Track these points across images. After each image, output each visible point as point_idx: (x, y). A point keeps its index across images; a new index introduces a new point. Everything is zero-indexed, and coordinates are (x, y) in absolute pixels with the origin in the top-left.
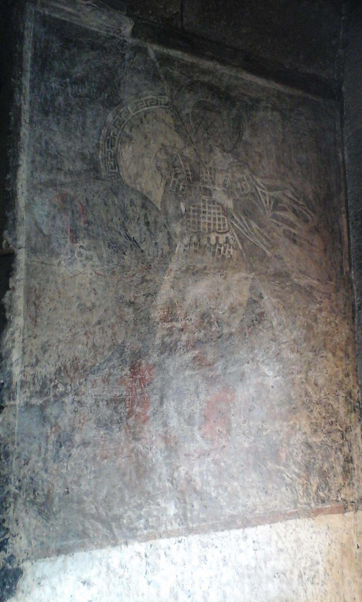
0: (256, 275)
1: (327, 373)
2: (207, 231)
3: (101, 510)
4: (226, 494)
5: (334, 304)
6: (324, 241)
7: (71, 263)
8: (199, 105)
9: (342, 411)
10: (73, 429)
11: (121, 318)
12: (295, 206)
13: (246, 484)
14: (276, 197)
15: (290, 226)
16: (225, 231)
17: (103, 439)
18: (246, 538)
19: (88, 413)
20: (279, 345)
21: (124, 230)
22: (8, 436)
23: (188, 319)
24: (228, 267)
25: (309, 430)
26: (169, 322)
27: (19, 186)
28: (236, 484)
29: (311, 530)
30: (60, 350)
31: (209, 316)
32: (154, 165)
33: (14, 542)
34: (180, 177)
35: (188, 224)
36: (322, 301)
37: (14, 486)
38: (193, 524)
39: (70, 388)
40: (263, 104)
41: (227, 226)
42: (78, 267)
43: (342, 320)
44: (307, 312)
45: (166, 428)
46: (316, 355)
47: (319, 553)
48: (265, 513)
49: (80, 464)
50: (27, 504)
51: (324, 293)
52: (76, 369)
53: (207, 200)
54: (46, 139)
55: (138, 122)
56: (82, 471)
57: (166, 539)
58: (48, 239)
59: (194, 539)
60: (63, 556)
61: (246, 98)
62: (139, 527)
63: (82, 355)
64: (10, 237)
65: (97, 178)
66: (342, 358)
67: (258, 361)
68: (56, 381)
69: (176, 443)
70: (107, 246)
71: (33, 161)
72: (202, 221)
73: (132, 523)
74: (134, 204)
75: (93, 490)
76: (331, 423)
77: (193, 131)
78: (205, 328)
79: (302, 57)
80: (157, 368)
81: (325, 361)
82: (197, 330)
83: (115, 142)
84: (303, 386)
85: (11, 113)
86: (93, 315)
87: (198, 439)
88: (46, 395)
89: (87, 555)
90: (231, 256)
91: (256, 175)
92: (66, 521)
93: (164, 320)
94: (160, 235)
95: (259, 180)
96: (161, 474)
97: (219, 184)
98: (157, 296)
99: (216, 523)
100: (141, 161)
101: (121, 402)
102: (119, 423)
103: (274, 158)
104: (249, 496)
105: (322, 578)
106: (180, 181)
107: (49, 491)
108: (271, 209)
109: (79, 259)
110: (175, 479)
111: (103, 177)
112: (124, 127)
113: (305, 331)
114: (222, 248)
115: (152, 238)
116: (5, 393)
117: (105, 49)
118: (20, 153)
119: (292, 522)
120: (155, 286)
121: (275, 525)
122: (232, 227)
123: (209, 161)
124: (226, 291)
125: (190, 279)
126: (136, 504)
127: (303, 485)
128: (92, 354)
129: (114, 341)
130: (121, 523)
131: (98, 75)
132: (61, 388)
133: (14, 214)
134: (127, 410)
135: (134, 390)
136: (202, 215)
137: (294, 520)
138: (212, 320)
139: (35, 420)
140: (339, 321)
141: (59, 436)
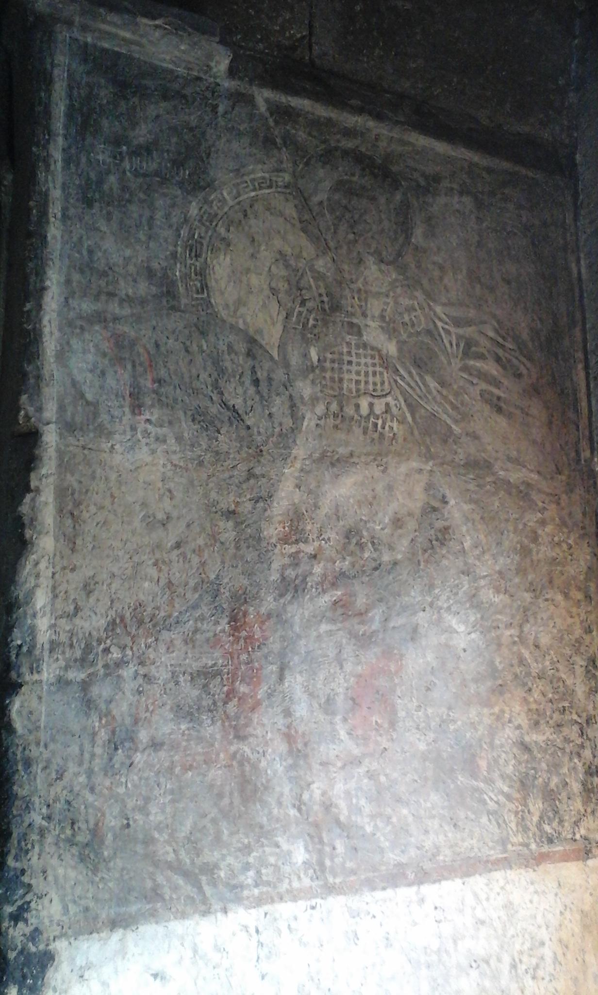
2: (354, 394)
3: (183, 854)
4: (389, 828)
5: (565, 513)
6: (548, 408)
7: (132, 448)
8: (339, 186)
9: (581, 690)
10: (136, 722)
11: (214, 536)
12: (500, 352)
13: (422, 812)
14: (467, 336)
15: (491, 384)
17: (186, 738)
20: (475, 580)
21: (218, 393)
22: (30, 731)
23: (323, 539)
25: (526, 721)
26: (292, 543)
27: (45, 321)
28: (405, 811)
29: (532, 889)
32: (266, 287)
33: (40, 907)
34: (309, 304)
35: (324, 382)
36: (544, 508)
37: (40, 814)
38: (334, 877)
39: (130, 653)
40: (445, 184)
42: (143, 454)
43: (579, 538)
44: (521, 527)
45: (290, 720)
46: (536, 597)
47: (544, 928)
48: (453, 861)
49: (147, 779)
50: (61, 845)
51: (548, 494)
52: (141, 623)
54: (89, 246)
55: (240, 215)
57: (290, 904)
58: (93, 407)
59: (336, 903)
60: (121, 931)
61: (416, 175)
62: (246, 882)
63: (151, 598)
64: (32, 406)
65: (173, 308)
66: (579, 601)
67: (441, 608)
68: (108, 641)
69: (306, 744)
71: (68, 282)
72: (346, 376)
75: (169, 821)
77: (330, 229)
78: (352, 554)
79: (508, 105)
80: (273, 620)
81: (552, 607)
83: (201, 248)
84: (515, 648)
85: (31, 203)
86: (168, 534)
87: (342, 738)
90: (394, 434)
91: (434, 301)
92: (125, 872)
93: (285, 540)
94: (278, 401)
95: (439, 309)
96: (282, 794)
97: (373, 317)
100: (244, 279)
101: (214, 676)
103: (464, 271)
104: (426, 832)
105: (550, 968)
106: (310, 311)
107: (96, 825)
108: (460, 355)
109: (144, 441)
110: (305, 804)
112: (216, 225)
113: (517, 558)
114: (380, 422)
115: (264, 406)
116: (24, 661)
117: (184, 97)
118: (47, 269)
119: (498, 875)
120: (269, 484)
121: (471, 880)
122: (394, 387)
123: (357, 280)
124: (386, 493)
125: (326, 473)
126: (240, 845)
127: (516, 813)
128: (166, 596)
129: (203, 576)
130: (215, 876)
131: (174, 140)
132: (116, 654)
133: (38, 367)
134: (225, 689)
135: (236, 656)
137: (503, 871)
138: (363, 540)
139: (73, 706)
140: (575, 541)
141: (113, 732)
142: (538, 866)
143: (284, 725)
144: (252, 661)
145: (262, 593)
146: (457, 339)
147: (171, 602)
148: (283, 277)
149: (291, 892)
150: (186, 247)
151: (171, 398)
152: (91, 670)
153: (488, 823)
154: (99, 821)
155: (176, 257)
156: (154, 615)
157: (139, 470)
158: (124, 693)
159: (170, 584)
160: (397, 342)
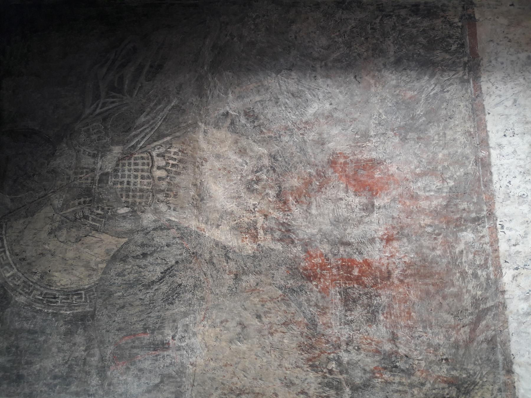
1: (315, 33)
2: (151, 180)
3: (466, 321)
4: (451, 168)
7: (192, 350)
9: (360, 15)
10: (377, 352)
11: (253, 290)
13: (441, 143)
16: (150, 157)
17: (389, 316)
18: (500, 145)
19: (360, 333)
21: (153, 285)
23: (254, 209)
24: (192, 155)
25: (380, 59)
26: (257, 232)
28: (440, 156)
29: (494, 62)
30: (290, 366)
32: (75, 246)
34: (87, 213)
35: (143, 204)
38: (483, 210)
39: (332, 354)
41: (145, 155)
42: (197, 341)
44: (244, 55)
45: (377, 239)
49: (416, 345)
52: (312, 347)
54: (51, 378)
55: (24, 263)
56: (423, 342)
57: (499, 244)
59: (500, 211)
62: (485, 276)
63: (295, 338)
65: (93, 316)
68: (325, 371)
69: (394, 228)
72: (139, 186)
73: (481, 285)
75: (444, 330)
76: (372, 30)
78: (264, 188)
80: (309, 248)
82: (266, 198)
83: (49, 294)
84: (330, 64)
86: (252, 325)
88: (341, 383)
89: (514, 339)
90: (180, 151)
92: (476, 362)
93: (255, 237)
94: (157, 240)
95: (88, 111)
96: (428, 248)
97: (94, 163)
98: (229, 247)
99: (483, 181)
100: (70, 262)
101: (347, 293)
102: (371, 296)
104: (454, 140)
107: (446, 382)
109: (187, 341)
110: (434, 230)
112: (32, 282)
114: (171, 162)
115: (161, 250)
120: (217, 248)
121: (487, 107)
123: (67, 175)
124: (221, 160)
125: (208, 205)
128: (294, 327)
129: (279, 299)
132: (333, 365)
134: (356, 286)
135: (334, 277)
138: (254, 179)
141: (385, 368)
142: (478, 57)
143: (380, 243)
144: (337, 265)
145: (291, 256)
146: (109, 97)
147: (298, 323)
148: (68, 232)
149: (492, 243)
150: (49, 305)
152: (344, 383)
153: (449, 93)
154: (443, 380)
155: (56, 313)
156: (306, 336)
157: (208, 345)
158: (359, 361)
159: (285, 324)
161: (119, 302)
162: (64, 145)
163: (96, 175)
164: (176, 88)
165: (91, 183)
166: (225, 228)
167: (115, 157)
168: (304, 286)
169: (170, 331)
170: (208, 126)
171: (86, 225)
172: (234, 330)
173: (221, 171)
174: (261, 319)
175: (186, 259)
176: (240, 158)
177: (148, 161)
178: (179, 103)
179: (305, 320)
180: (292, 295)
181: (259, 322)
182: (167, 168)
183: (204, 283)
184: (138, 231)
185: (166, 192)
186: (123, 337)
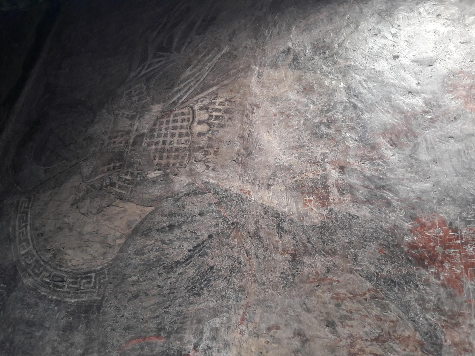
0: (255, 62)
2: (190, 137)
16: (191, 112)
21: (177, 267)
23: (323, 160)
24: (241, 103)
26: (327, 192)
31: (317, 126)
32: (95, 218)
34: (115, 179)
41: (186, 110)
53: (148, 140)
65: (99, 308)
70: (197, 298)
72: (175, 145)
74: (141, 250)
78: (339, 131)
86: (319, 337)
90: (226, 100)
95: (133, 74)
100: (87, 237)
108: (168, 54)
111: (99, 298)
112: (44, 261)
114: (215, 114)
115: (192, 221)
120: (266, 216)
123: (102, 140)
124: (277, 103)
136: (167, 147)
138: (325, 121)
148: (91, 202)
151: (177, 318)
155: (60, 301)
160: (152, 104)
161: (132, 289)
162: (105, 111)
163: (131, 137)
164: (229, 35)
165: (124, 146)
166: (278, 187)
167: (153, 116)
168: (413, 275)
169: (192, 337)
170: (263, 68)
171: (112, 193)
172: (288, 344)
173: (278, 117)
174: (334, 328)
175: (223, 232)
176: (305, 97)
177: (189, 116)
178: (230, 50)
179: (418, 335)
180: (391, 290)
181: (332, 333)
182: (210, 121)
183: (245, 265)
184: (167, 198)
185: (206, 149)
186: (131, 340)
